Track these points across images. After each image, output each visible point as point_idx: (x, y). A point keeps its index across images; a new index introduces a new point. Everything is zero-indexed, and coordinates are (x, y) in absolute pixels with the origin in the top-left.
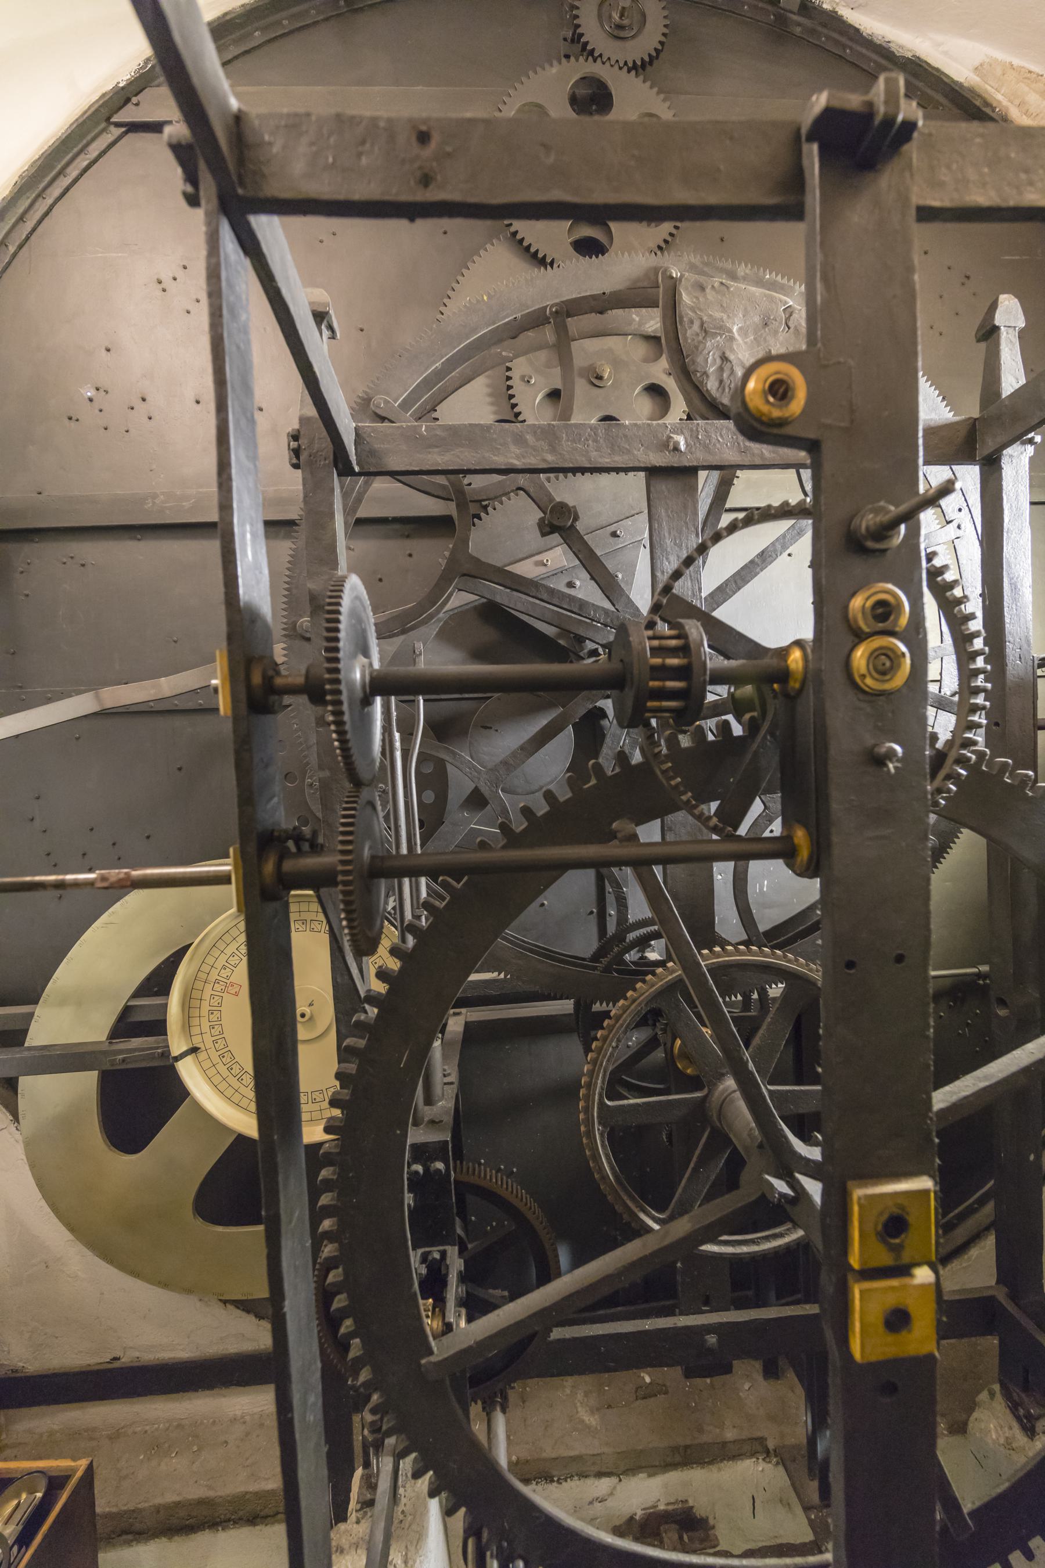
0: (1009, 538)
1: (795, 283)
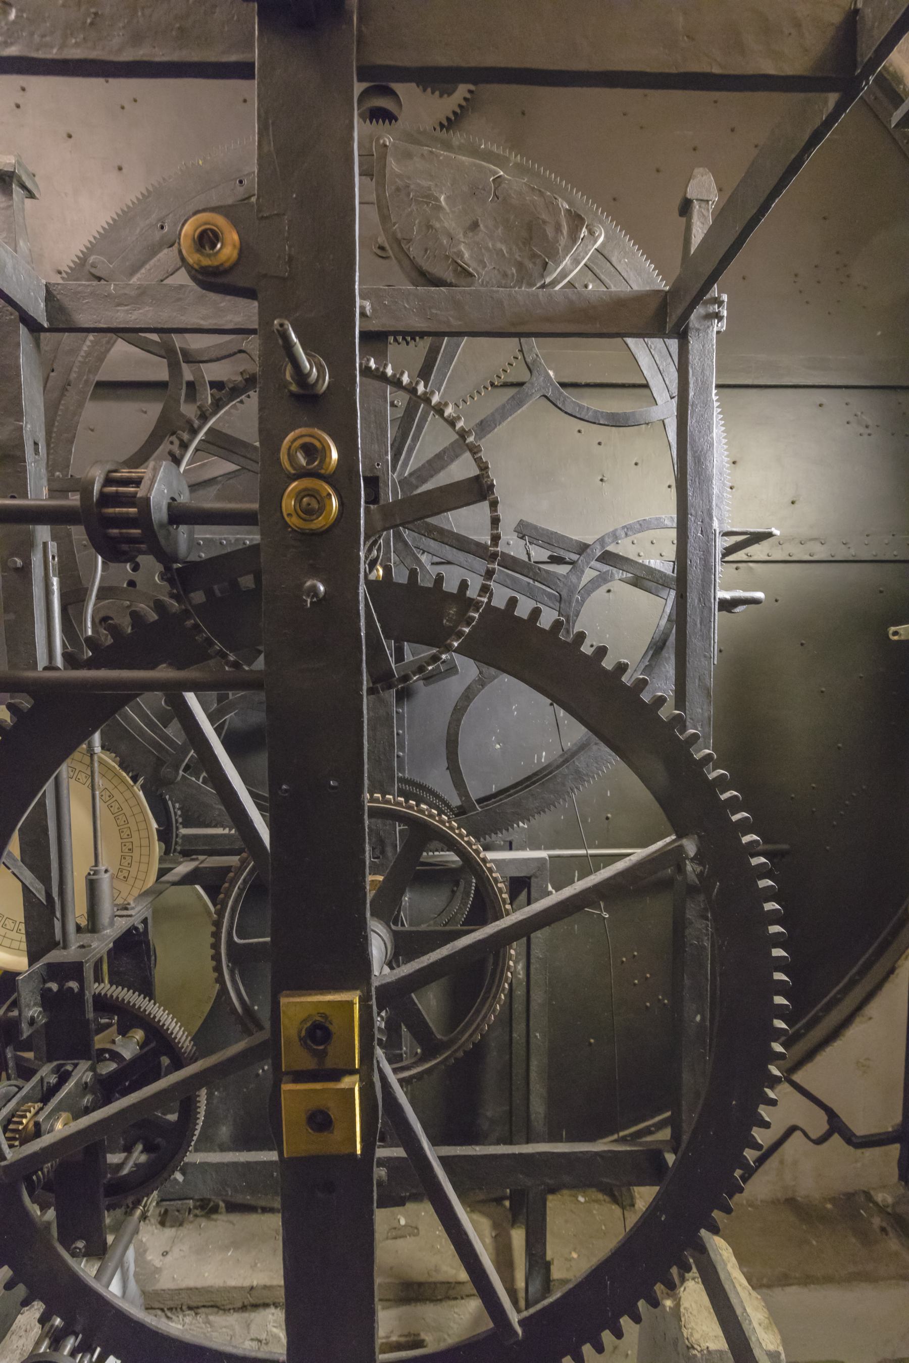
0: (693, 411)
1: (510, 153)
